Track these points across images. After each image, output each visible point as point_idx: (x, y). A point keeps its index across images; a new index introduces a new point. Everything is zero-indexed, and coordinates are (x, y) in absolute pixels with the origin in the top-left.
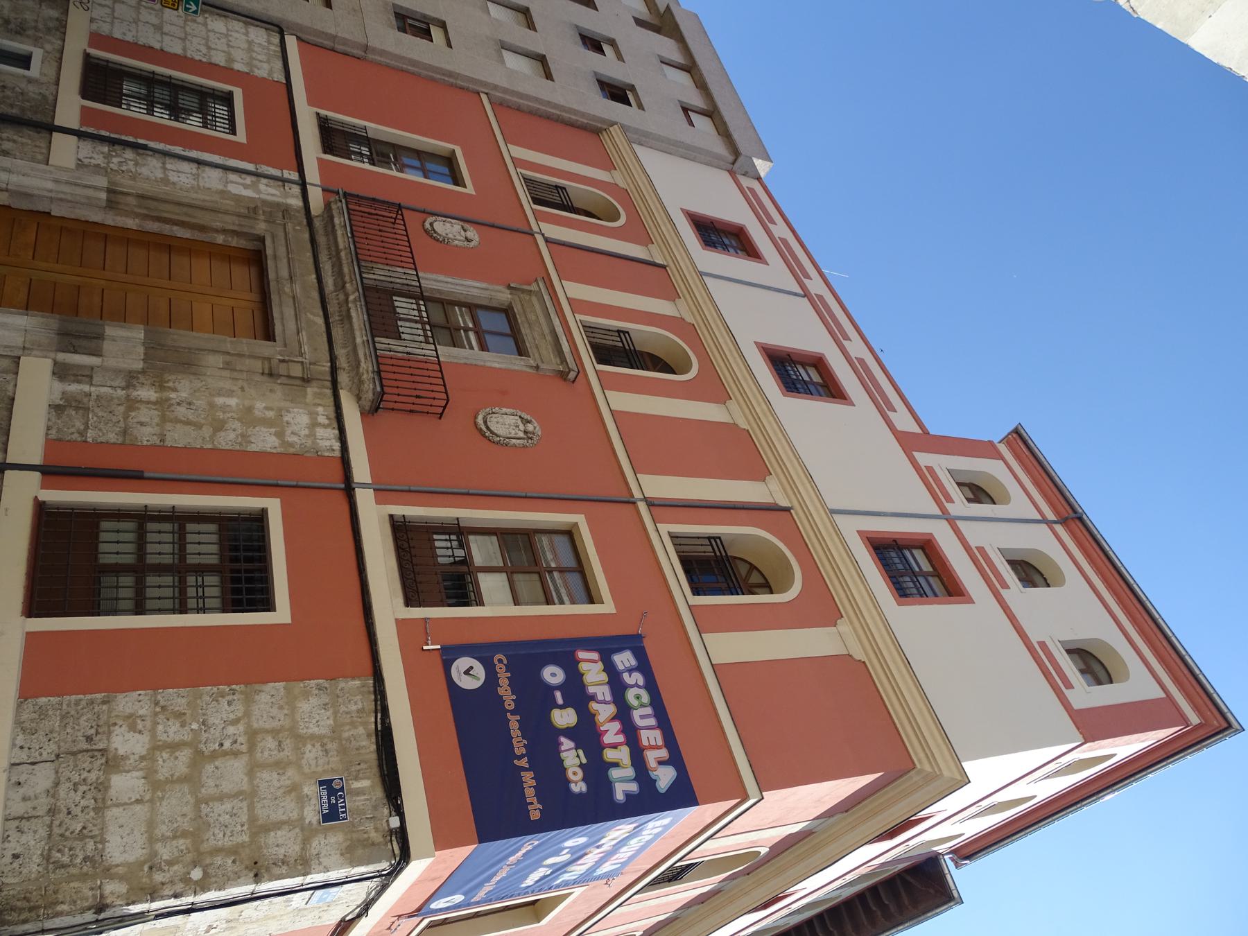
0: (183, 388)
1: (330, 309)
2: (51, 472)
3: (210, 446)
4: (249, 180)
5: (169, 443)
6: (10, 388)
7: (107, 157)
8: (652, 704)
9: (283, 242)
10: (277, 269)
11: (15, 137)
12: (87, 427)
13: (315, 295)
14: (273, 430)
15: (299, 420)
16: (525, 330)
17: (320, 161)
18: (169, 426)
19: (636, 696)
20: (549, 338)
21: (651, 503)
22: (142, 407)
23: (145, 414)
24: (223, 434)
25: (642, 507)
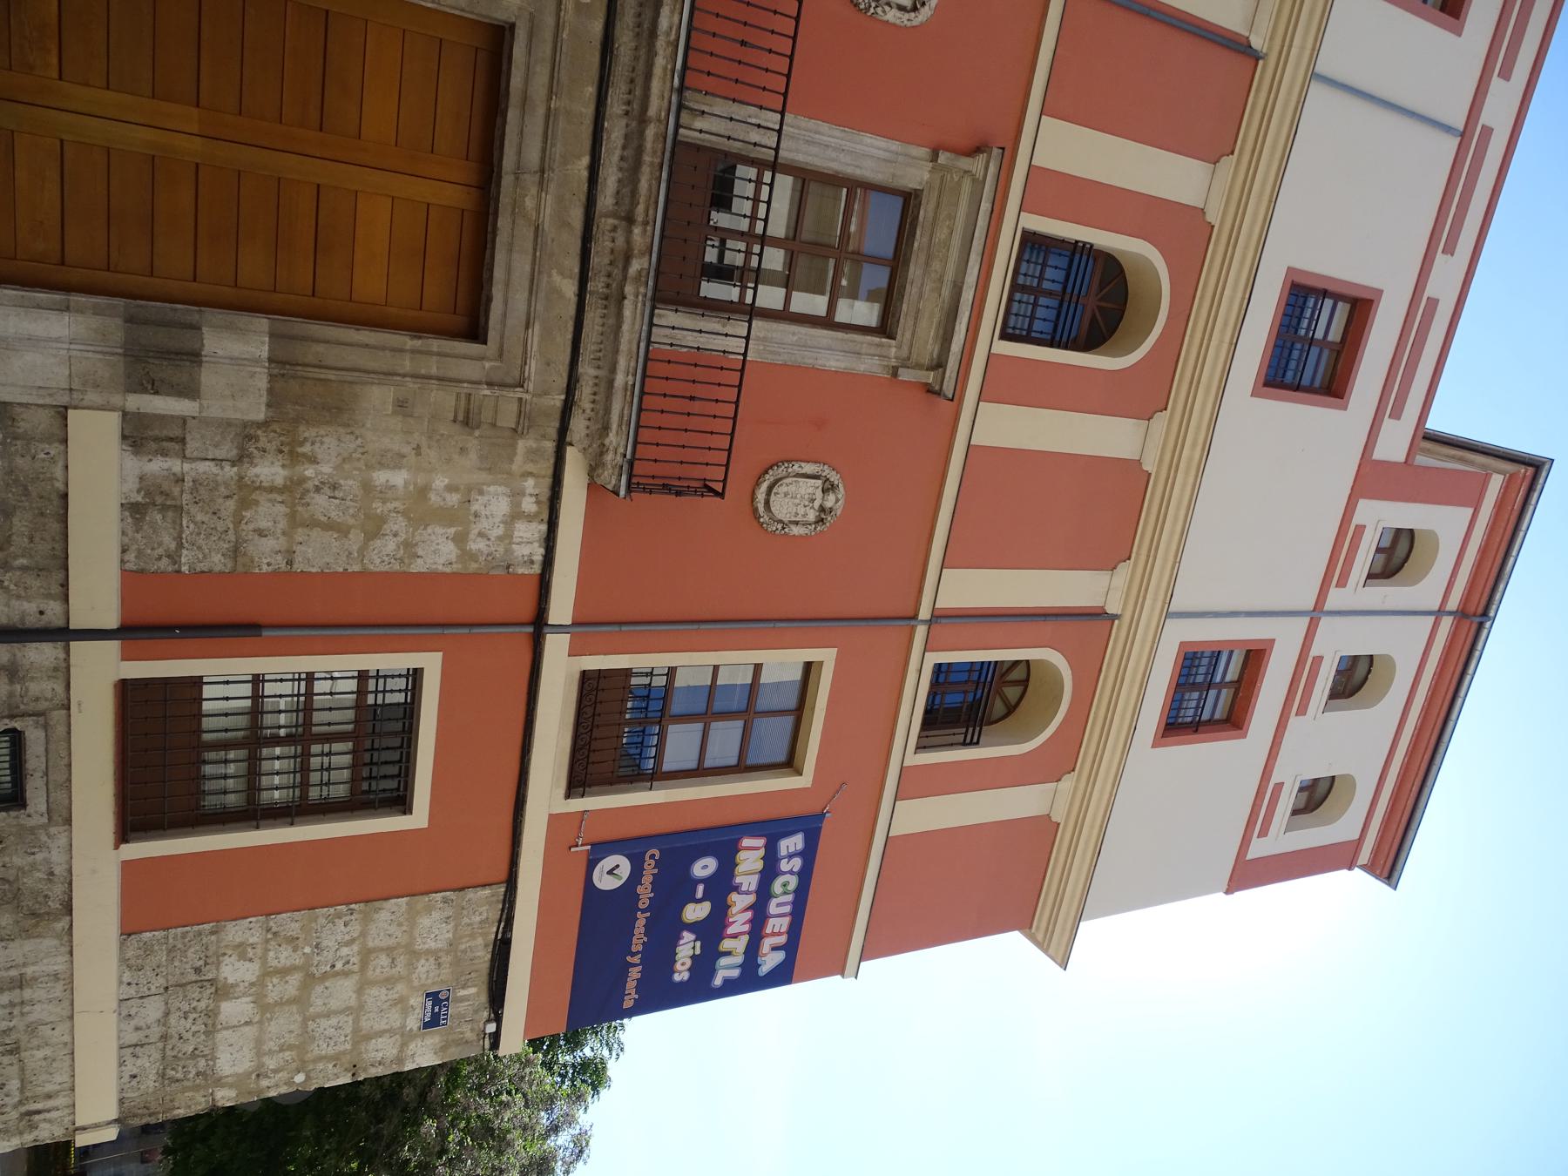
0: (328, 450)
1: (595, 260)
2: (134, 632)
3: (356, 568)
5: (298, 567)
6: (58, 472)
8: (794, 903)
9: (548, 52)
10: (527, 72)
12: (180, 546)
13: (576, 216)
14: (453, 530)
15: (494, 505)
16: (914, 271)
18: (300, 535)
19: (784, 885)
20: (946, 292)
22: (262, 497)
23: (268, 513)
24: (378, 543)
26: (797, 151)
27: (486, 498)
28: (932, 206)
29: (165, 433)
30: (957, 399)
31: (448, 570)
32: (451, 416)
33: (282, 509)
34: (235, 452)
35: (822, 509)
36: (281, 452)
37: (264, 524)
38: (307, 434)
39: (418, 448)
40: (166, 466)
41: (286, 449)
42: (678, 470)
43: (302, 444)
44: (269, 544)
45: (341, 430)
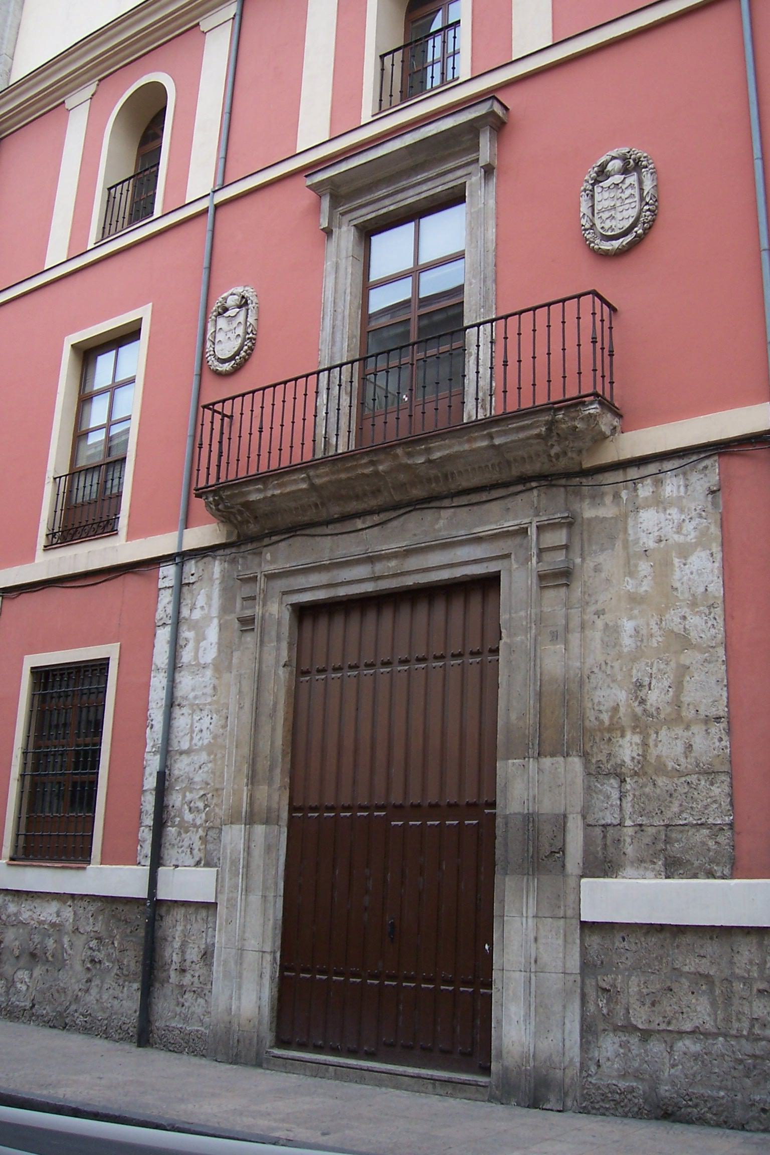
0: (609, 696)
3: (721, 651)
4: (187, 634)
5: (722, 710)
7: (184, 828)
11: (177, 944)
14: (676, 561)
17: (130, 536)
18: (688, 714)
22: (653, 752)
24: (693, 635)
29: (599, 841)
31: (719, 556)
32: (563, 590)
33: (663, 732)
34: (612, 781)
35: (625, 171)
36: (610, 739)
37: (679, 748)
38: (593, 719)
39: (598, 614)
40: (628, 840)
41: (607, 736)
43: (602, 722)
44: (699, 742)
45: (587, 687)
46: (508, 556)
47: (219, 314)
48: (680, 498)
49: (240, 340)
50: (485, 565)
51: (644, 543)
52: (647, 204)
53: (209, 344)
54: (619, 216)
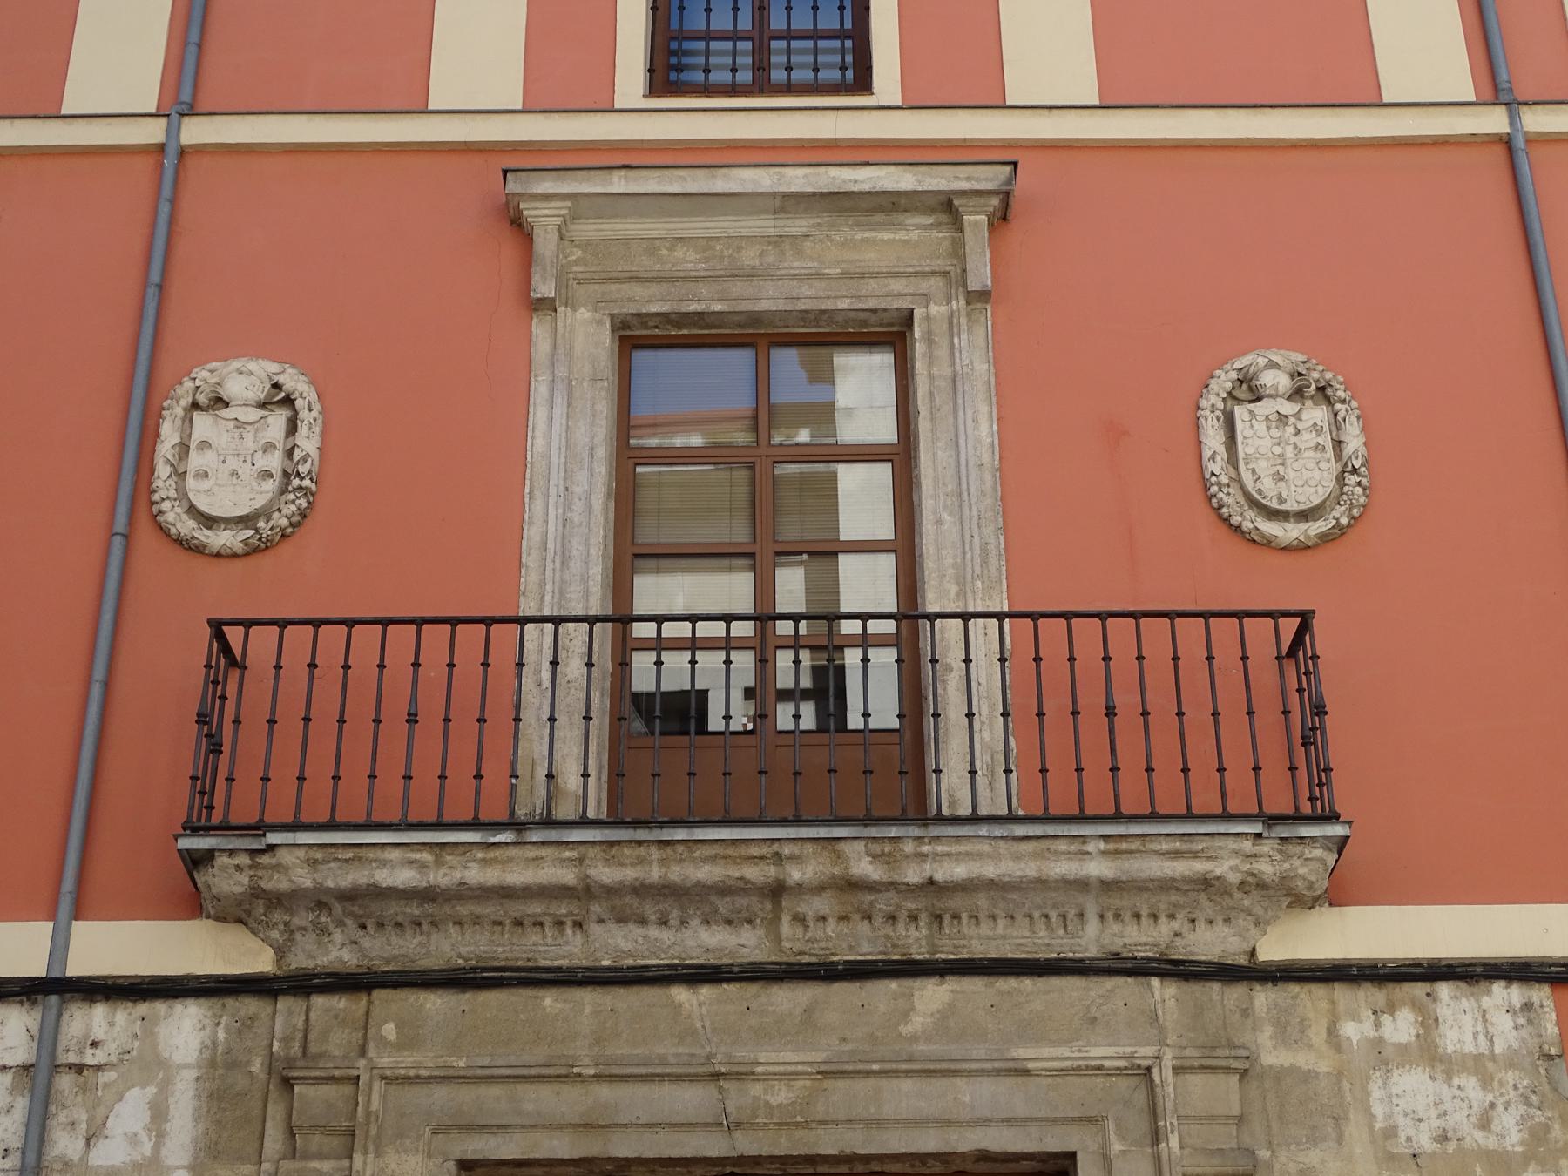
1: (867, 951)
9: (495, 1091)
13: (788, 998)
16: (769, 299)
20: (797, 225)
21: (181, 102)
25: (196, 131)
26: (585, 579)
27: (1401, 1121)
28: (638, 291)
30: (1009, 156)
35: (1298, 394)
42: (1268, 717)
46: (1089, 1120)
47: (195, 406)
48: (1478, 1058)
49: (270, 486)
50: (1034, 1131)
51: (1409, 1139)
52: (1355, 470)
53: (163, 470)
54: (1291, 475)
